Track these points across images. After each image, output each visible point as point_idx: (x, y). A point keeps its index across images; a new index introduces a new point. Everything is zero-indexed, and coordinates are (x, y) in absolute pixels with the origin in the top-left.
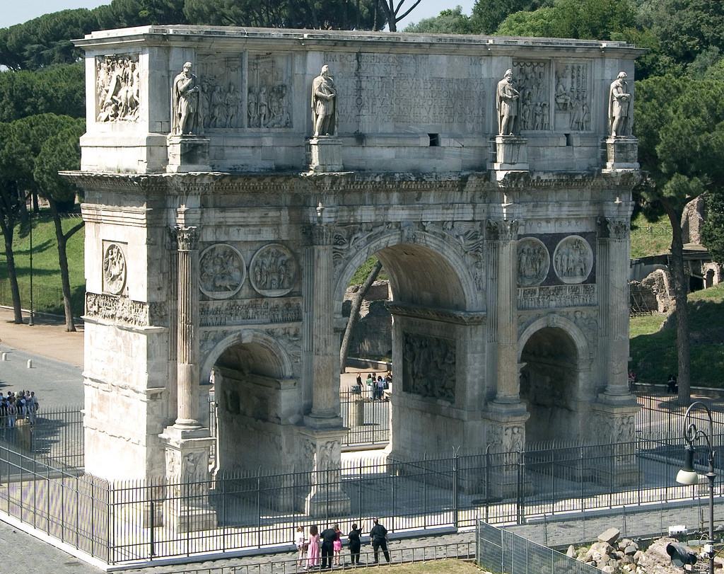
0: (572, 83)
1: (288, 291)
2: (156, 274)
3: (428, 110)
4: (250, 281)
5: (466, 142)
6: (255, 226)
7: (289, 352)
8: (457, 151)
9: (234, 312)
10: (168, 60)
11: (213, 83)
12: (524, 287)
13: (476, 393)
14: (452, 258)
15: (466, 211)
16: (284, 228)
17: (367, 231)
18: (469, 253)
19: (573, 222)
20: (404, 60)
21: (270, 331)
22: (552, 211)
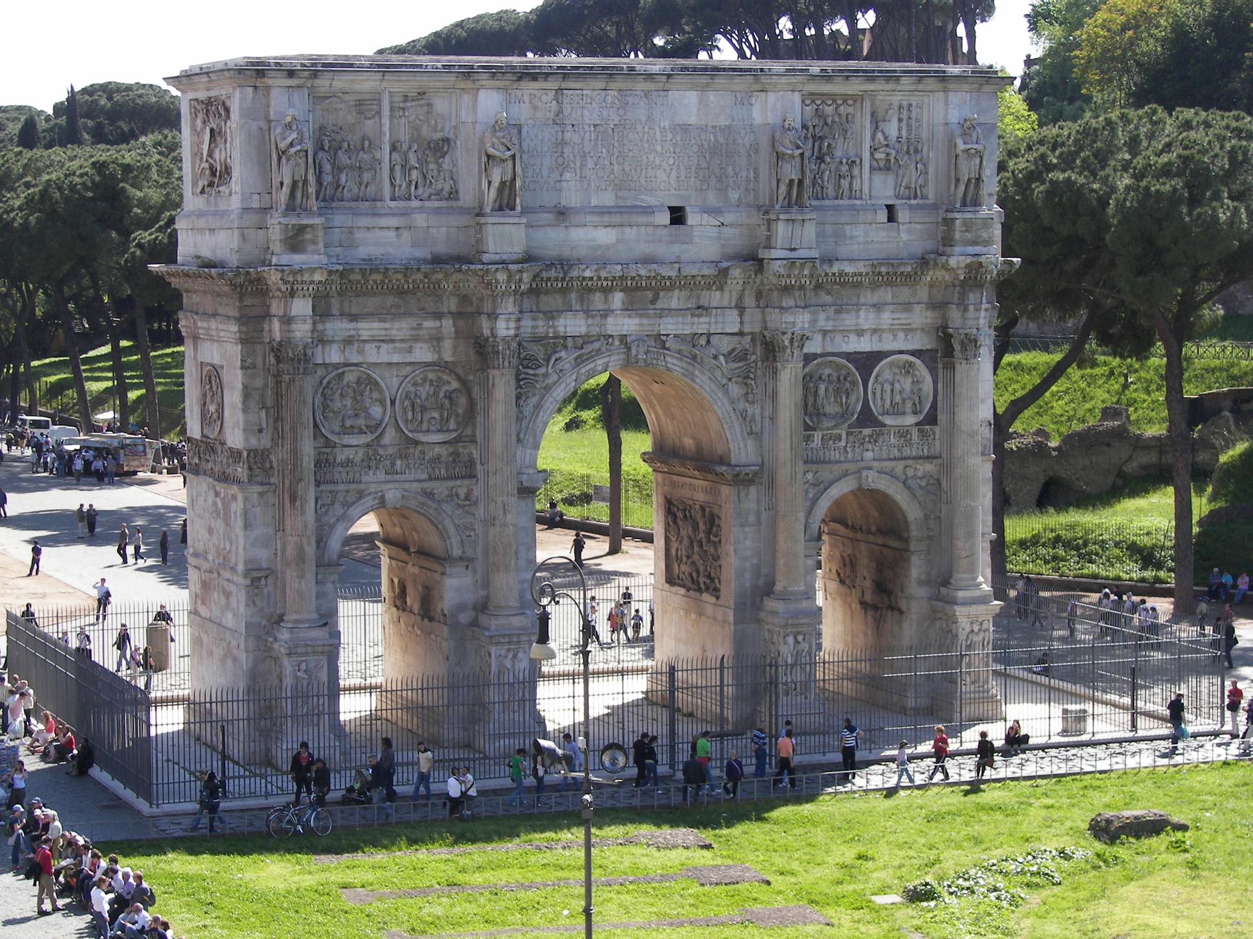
0: (900, 129)
1: (455, 435)
2: (256, 410)
3: (668, 169)
4: (396, 420)
5: (729, 218)
6: (402, 341)
7: (457, 521)
8: (713, 232)
9: (373, 464)
10: (268, 106)
11: (338, 138)
13: (748, 584)
14: (707, 389)
16: (447, 344)
17: (575, 348)
18: (733, 380)
19: (901, 335)
20: (630, 100)
22: (866, 319)
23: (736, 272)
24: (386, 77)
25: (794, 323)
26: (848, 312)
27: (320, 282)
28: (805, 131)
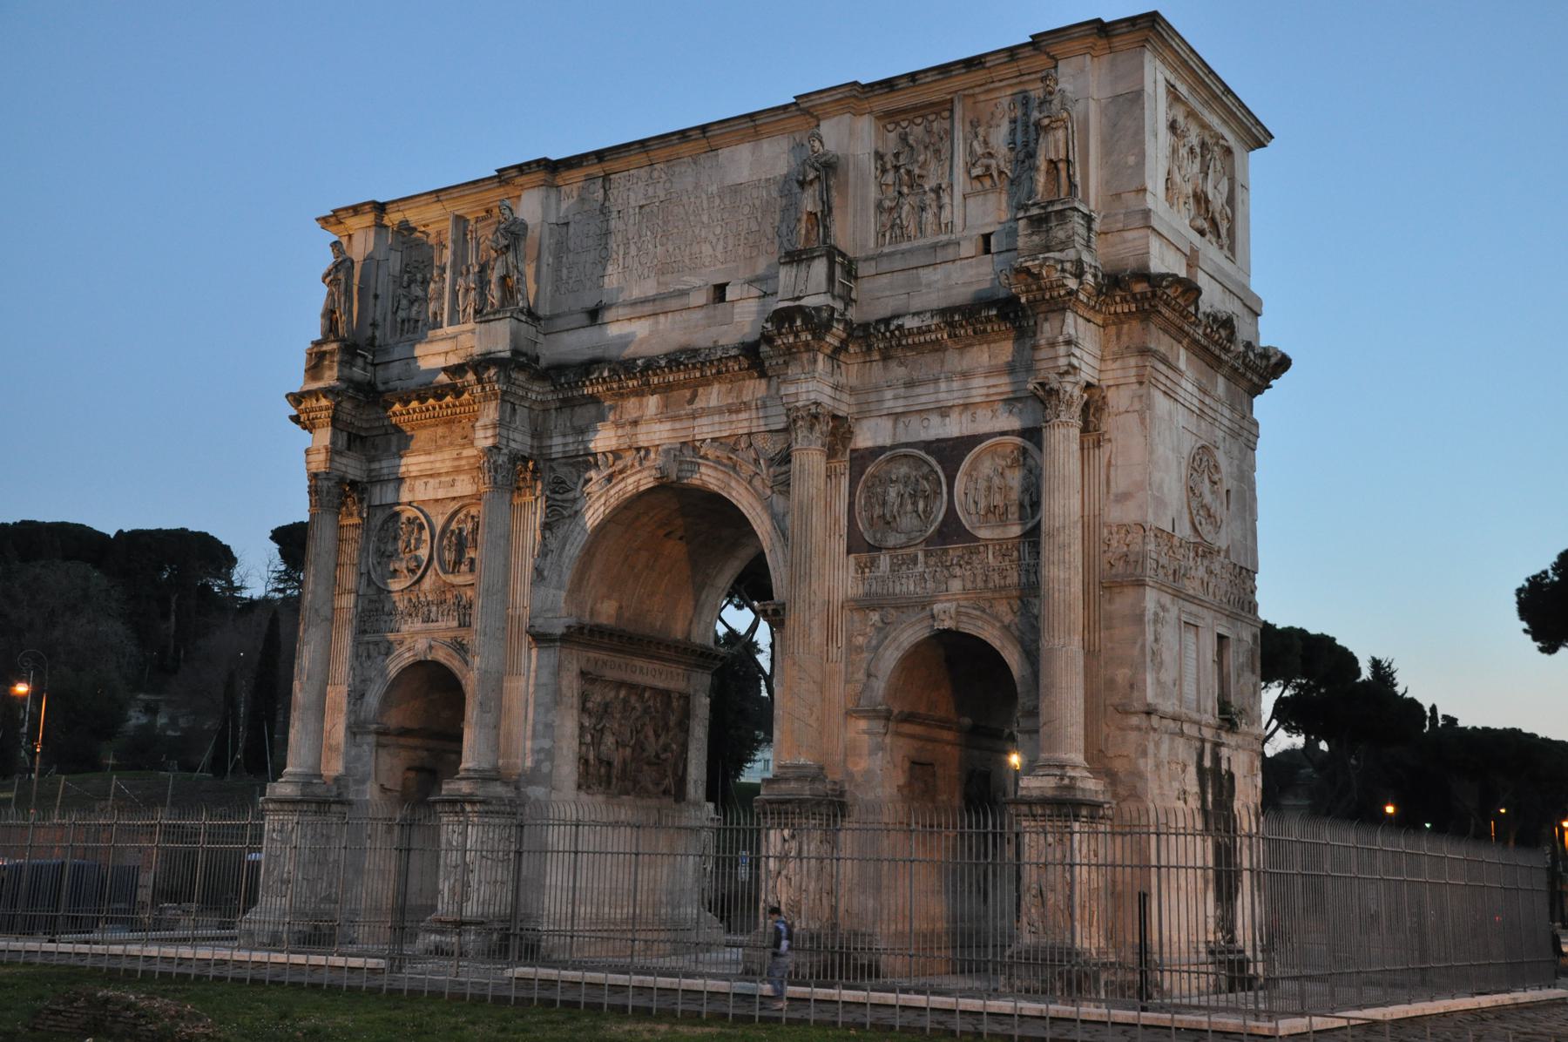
3: (714, 241)
12: (886, 549)
14: (745, 503)
15: (771, 411)
20: (677, 169)
21: (459, 640)
22: (948, 393)
23: (764, 348)
24: (441, 198)
25: (797, 393)
26: (922, 383)
27: (327, 408)
28: (879, 162)
